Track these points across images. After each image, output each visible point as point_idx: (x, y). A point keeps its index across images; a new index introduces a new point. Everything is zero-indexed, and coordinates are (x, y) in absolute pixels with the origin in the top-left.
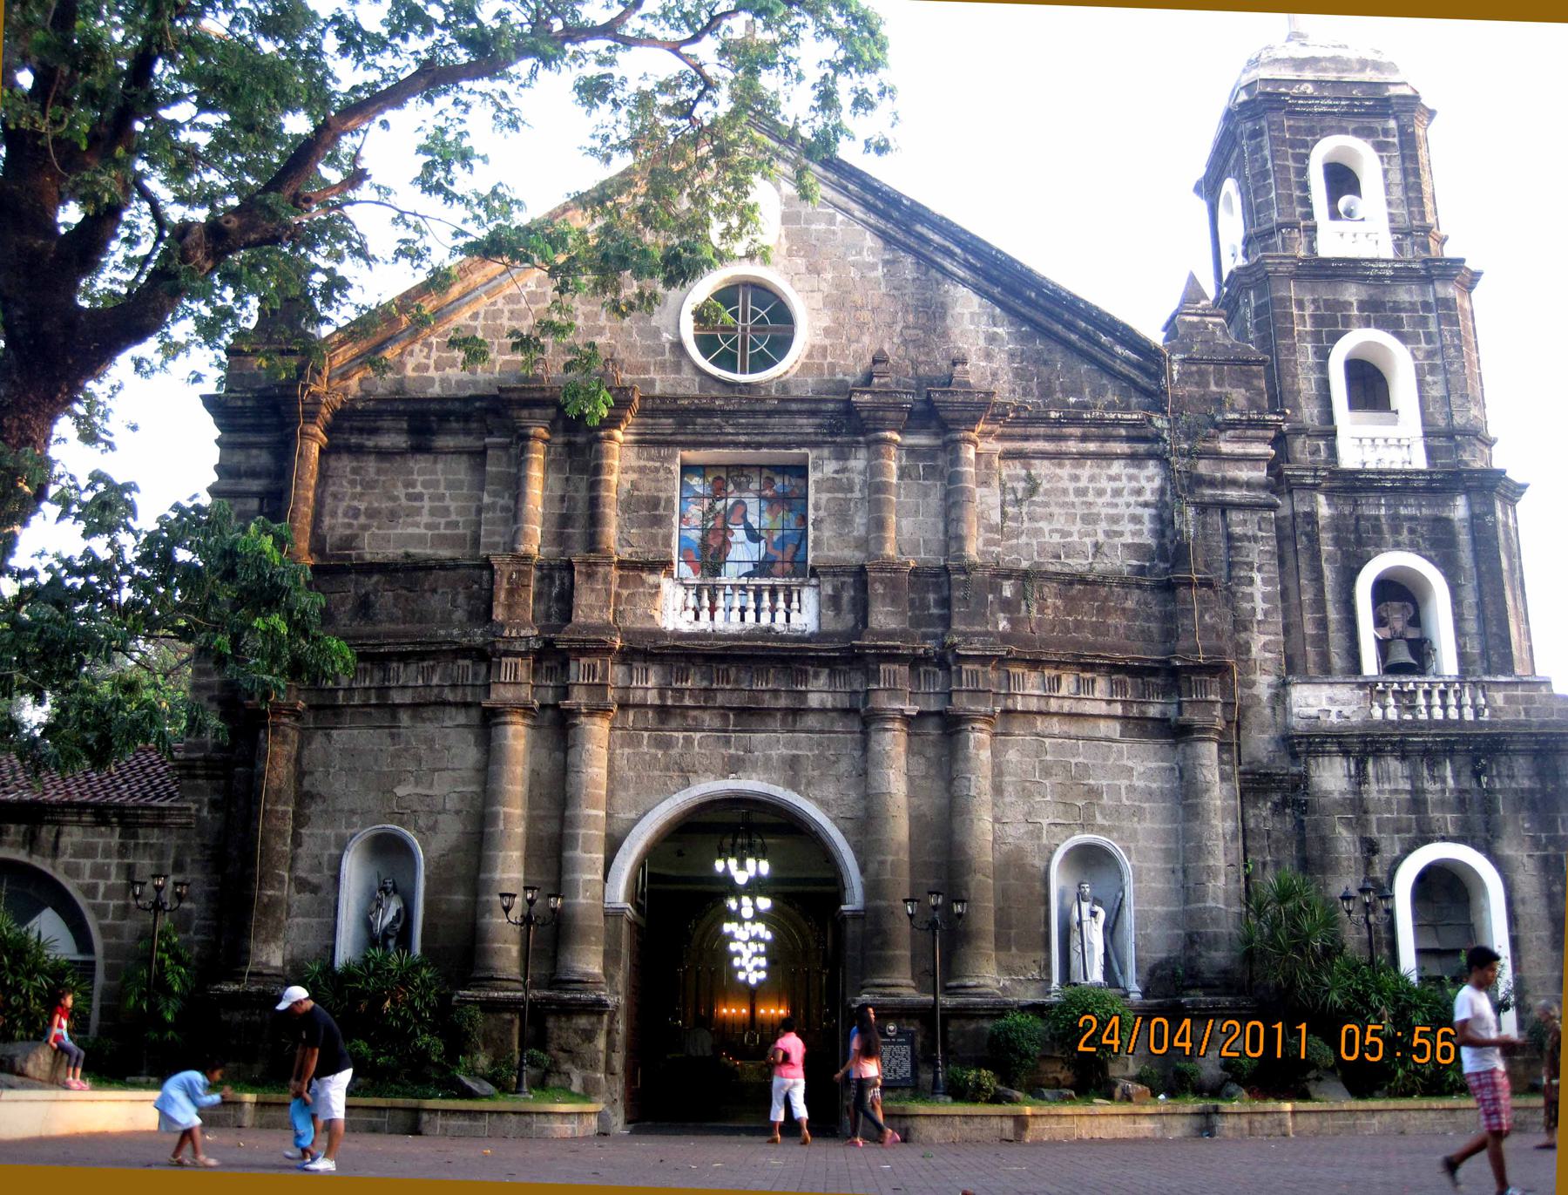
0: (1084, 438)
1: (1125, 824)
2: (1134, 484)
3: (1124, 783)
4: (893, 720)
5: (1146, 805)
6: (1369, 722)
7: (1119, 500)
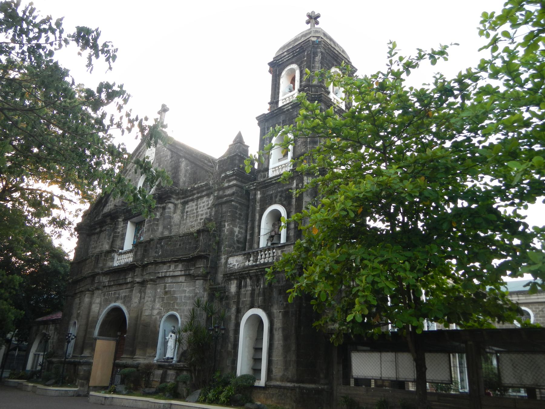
0: (198, 193)
2: (207, 203)
3: (183, 295)
4: (135, 283)
5: (188, 301)
6: (244, 267)
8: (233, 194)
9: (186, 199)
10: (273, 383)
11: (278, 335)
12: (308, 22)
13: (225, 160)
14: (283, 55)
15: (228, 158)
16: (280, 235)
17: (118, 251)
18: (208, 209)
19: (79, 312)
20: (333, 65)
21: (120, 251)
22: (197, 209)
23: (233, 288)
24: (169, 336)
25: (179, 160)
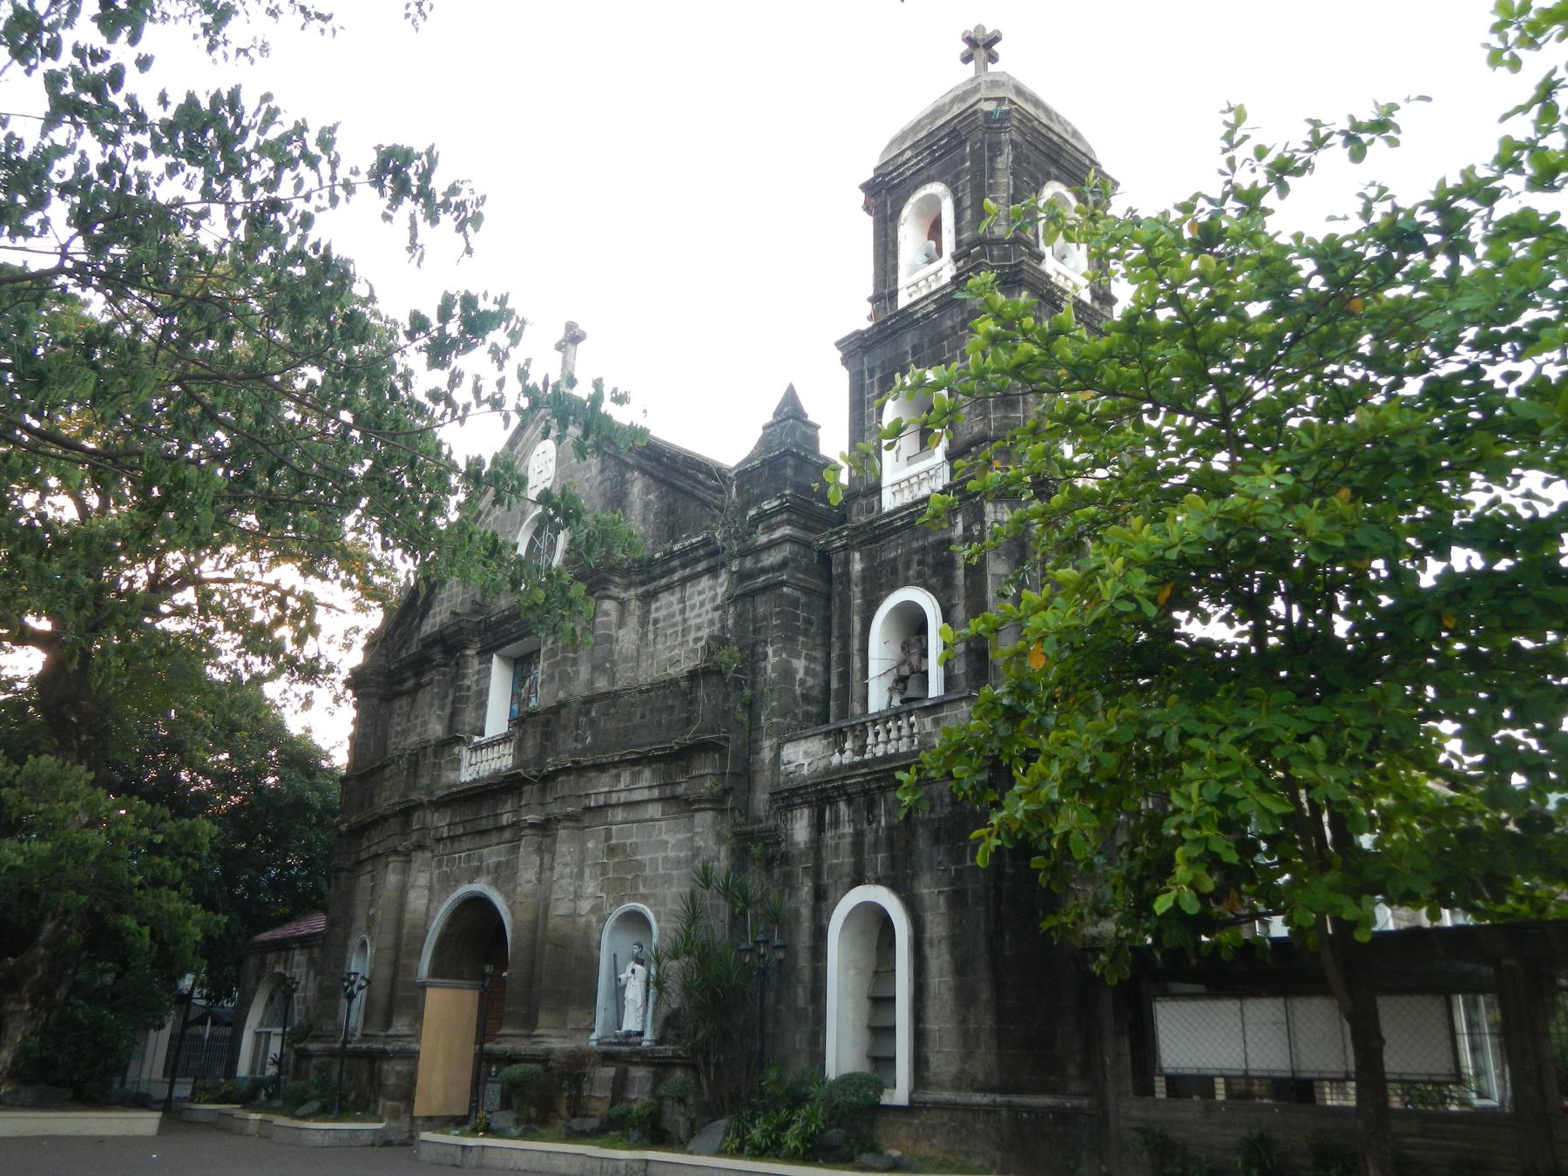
0: (684, 566)
1: (658, 890)
6: (828, 771)
7: (703, 610)
8: (783, 565)
9: (651, 587)
10: (932, 1095)
11: (939, 960)
12: (966, 59)
13: (754, 469)
14: (901, 160)
15: (763, 463)
16: (926, 673)
17: (471, 739)
18: (716, 609)
19: (371, 912)
20: (1048, 177)
21: (476, 739)
22: (683, 612)
23: (801, 830)
24: (629, 970)
25: (623, 475)
